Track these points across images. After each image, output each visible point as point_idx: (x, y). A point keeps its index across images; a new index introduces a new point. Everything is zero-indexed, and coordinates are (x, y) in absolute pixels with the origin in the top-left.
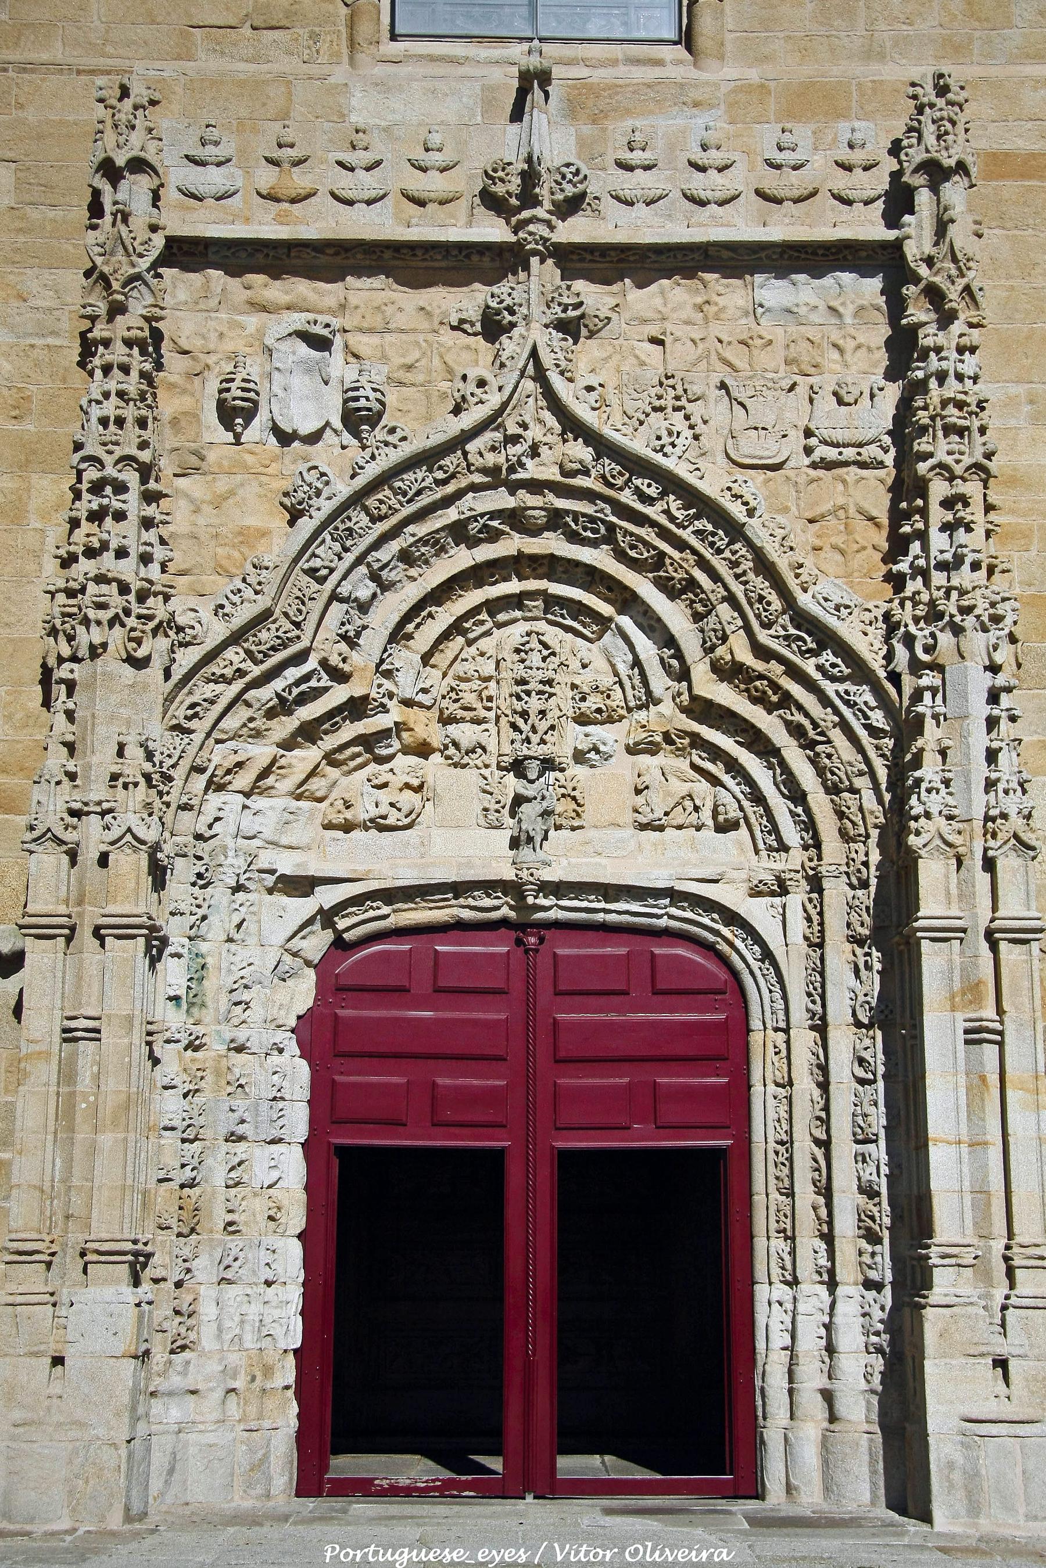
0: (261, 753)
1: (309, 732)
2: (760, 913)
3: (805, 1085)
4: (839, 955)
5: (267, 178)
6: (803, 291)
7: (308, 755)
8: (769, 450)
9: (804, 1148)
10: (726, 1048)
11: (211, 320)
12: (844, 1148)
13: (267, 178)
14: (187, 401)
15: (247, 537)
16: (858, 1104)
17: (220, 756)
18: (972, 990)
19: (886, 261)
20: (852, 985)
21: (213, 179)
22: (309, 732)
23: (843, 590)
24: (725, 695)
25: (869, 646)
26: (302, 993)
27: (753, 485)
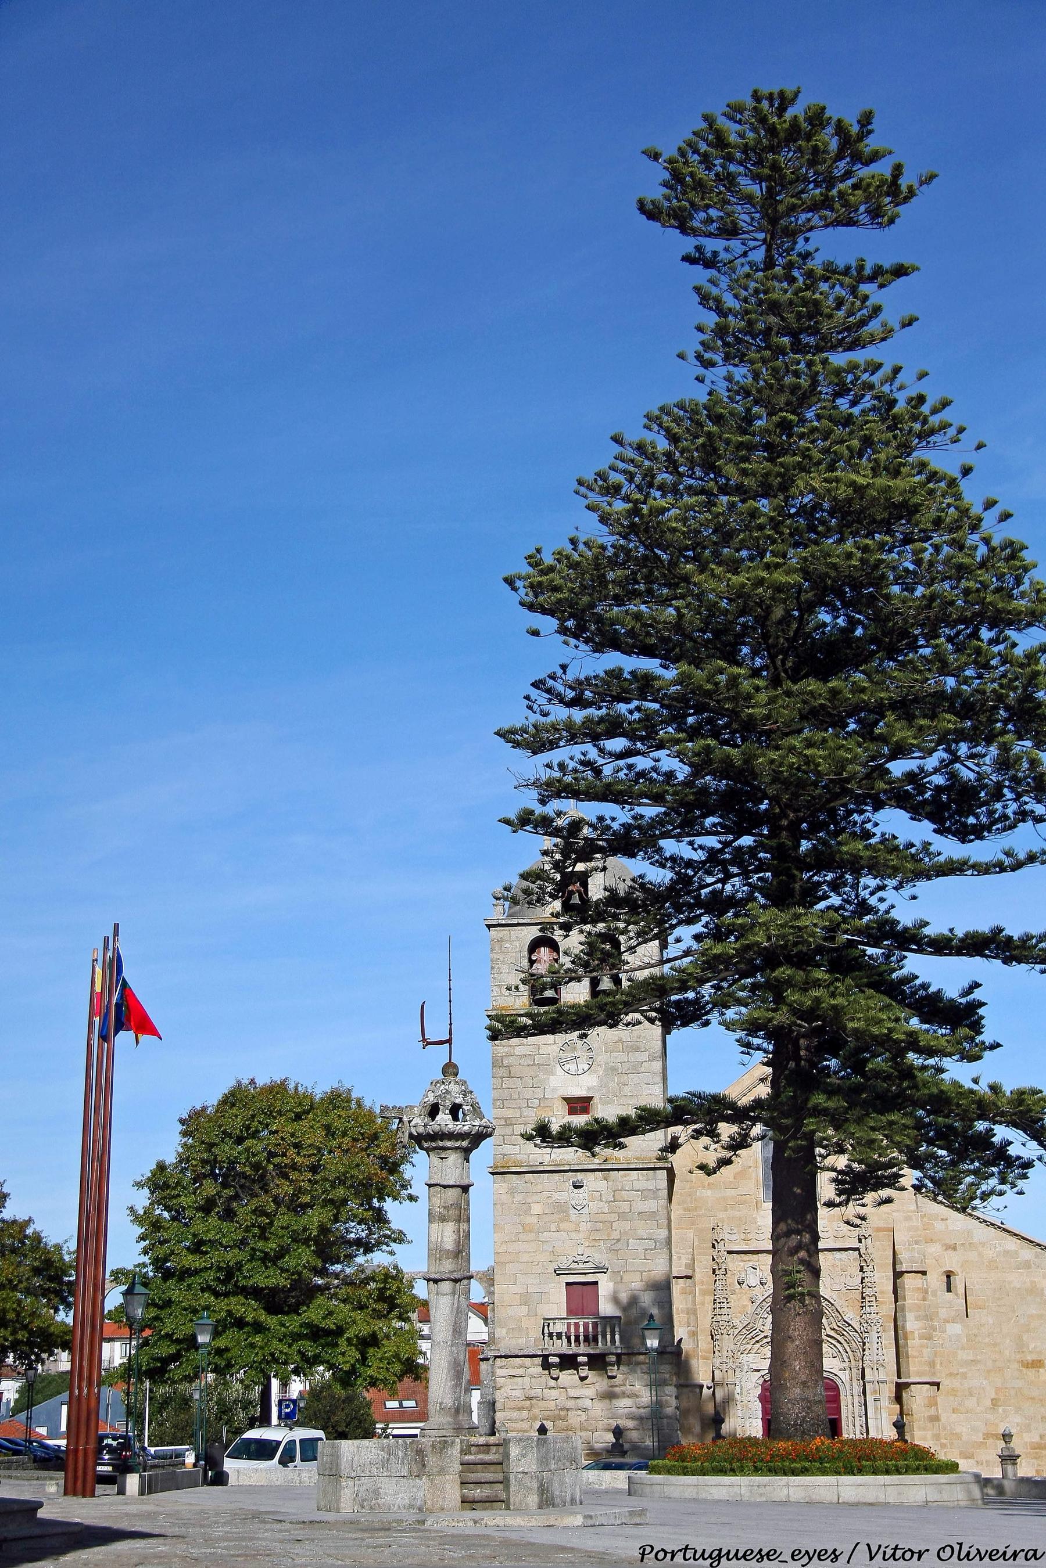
0: (749, 1346)
1: (757, 1342)
2: (840, 1374)
3: (850, 1406)
4: (855, 1383)
5: (743, 1236)
6: (844, 1254)
7: (758, 1345)
8: (838, 1287)
9: (850, 1418)
10: (838, 1395)
11: (735, 1264)
12: (857, 1418)
13: (743, 1236)
14: (732, 1280)
15: (744, 1306)
16: (859, 1410)
17: (742, 1348)
18: (875, 1392)
19: (858, 1249)
20: (857, 1389)
21: (734, 1237)
22: (757, 1342)
23: (851, 1315)
24: (832, 1333)
25: (857, 1326)
26: (759, 1391)
27: (835, 1295)
